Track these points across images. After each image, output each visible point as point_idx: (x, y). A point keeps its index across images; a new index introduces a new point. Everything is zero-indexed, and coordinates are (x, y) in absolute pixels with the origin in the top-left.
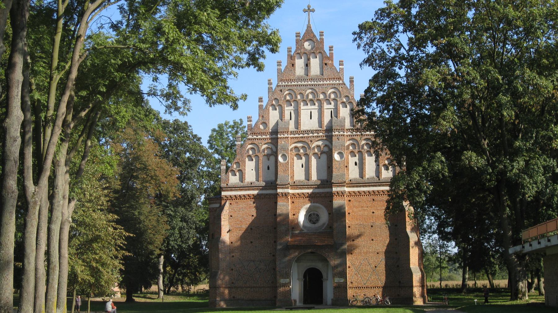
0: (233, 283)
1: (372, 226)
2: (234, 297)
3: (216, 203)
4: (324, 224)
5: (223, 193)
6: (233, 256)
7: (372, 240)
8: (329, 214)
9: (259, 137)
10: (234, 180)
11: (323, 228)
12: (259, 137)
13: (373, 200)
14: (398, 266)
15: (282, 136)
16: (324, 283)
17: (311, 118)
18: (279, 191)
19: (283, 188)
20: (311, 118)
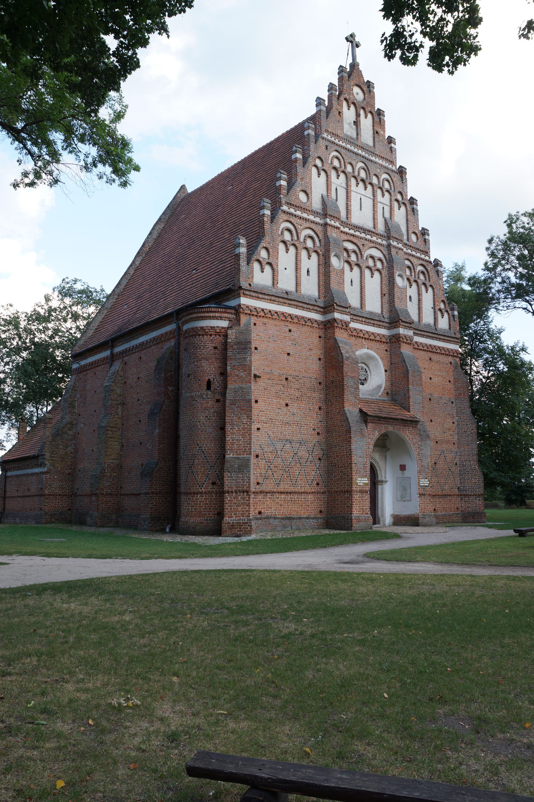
0: (258, 483)
1: (430, 399)
2: (260, 513)
3: (221, 318)
4: (380, 387)
5: (244, 301)
6: (258, 429)
7: (431, 421)
8: (386, 371)
9: (298, 213)
10: (261, 278)
11: (380, 394)
12: (298, 213)
13: (430, 359)
14: (456, 464)
15: (332, 223)
16: (380, 487)
17: (361, 210)
18: (337, 315)
19: (342, 313)
20: (361, 210)
